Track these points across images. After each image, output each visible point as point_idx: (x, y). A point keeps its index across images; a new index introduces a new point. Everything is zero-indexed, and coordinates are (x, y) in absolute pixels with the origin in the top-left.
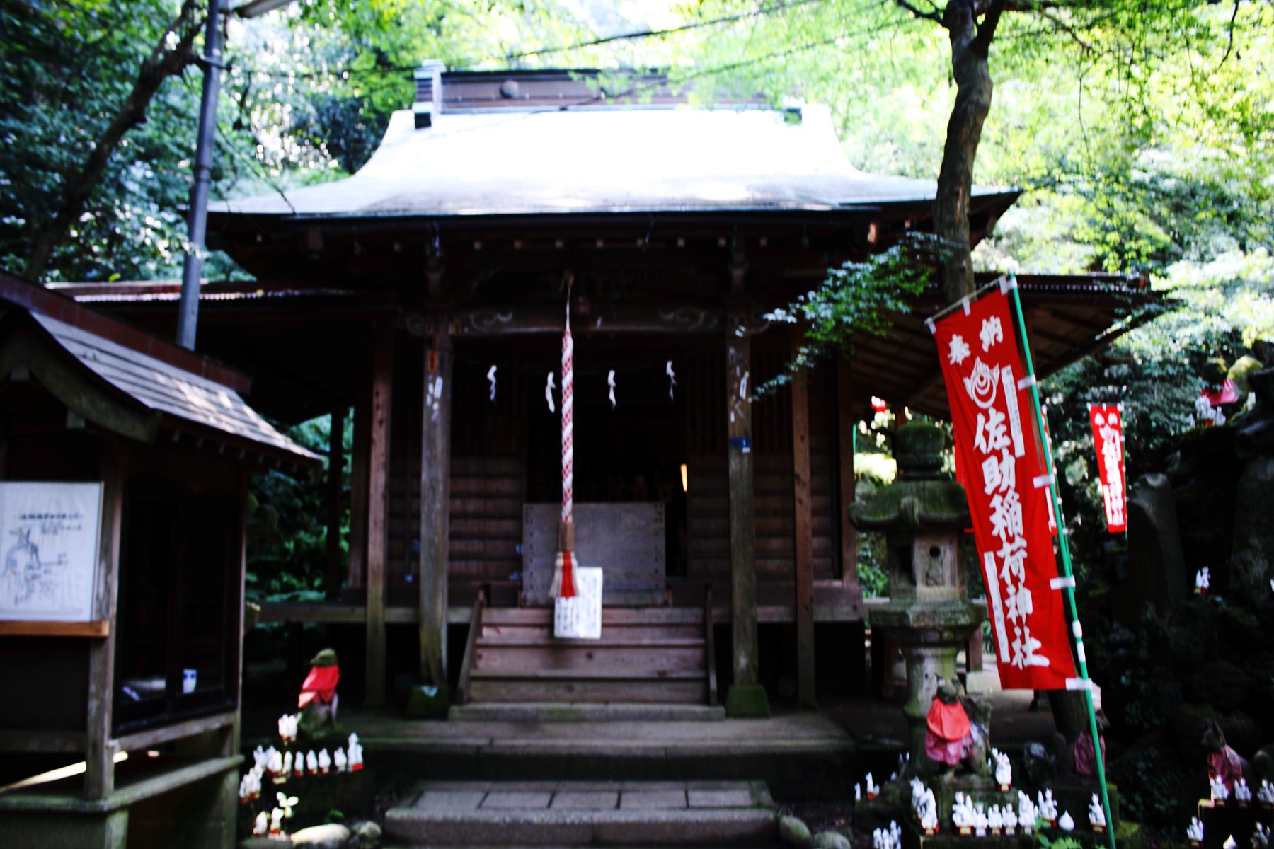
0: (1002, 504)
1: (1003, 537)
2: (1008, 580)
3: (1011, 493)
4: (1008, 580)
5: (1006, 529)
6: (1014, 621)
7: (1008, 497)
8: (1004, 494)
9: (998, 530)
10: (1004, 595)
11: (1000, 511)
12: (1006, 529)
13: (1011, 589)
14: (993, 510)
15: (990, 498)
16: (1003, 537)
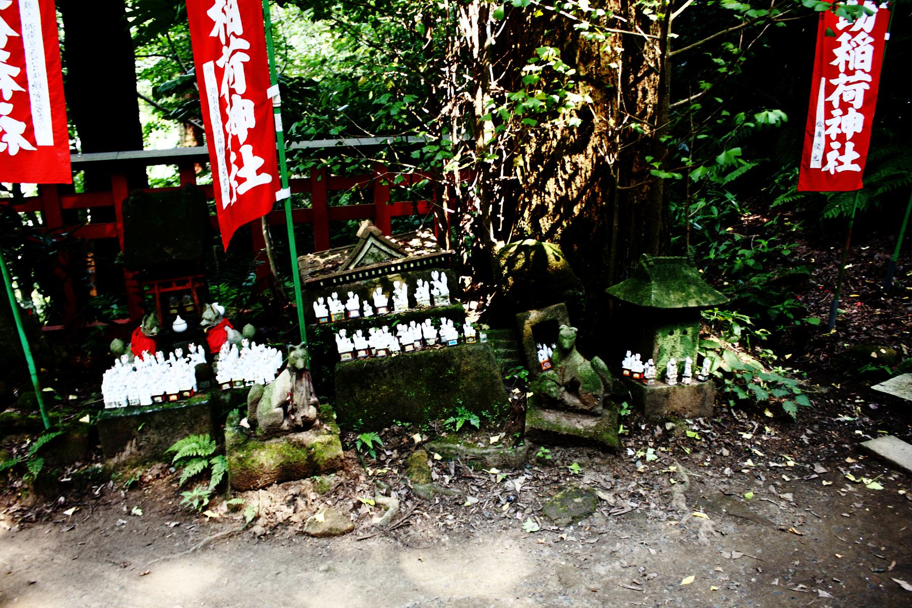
0: (849, 42)
1: (842, 68)
2: (836, 104)
3: (862, 35)
4: (836, 104)
5: (847, 63)
6: (833, 137)
7: (858, 38)
8: (854, 34)
9: (839, 61)
10: (828, 116)
11: (845, 47)
12: (847, 63)
13: (837, 112)
14: (839, 45)
15: (840, 33)
16: (842, 68)
